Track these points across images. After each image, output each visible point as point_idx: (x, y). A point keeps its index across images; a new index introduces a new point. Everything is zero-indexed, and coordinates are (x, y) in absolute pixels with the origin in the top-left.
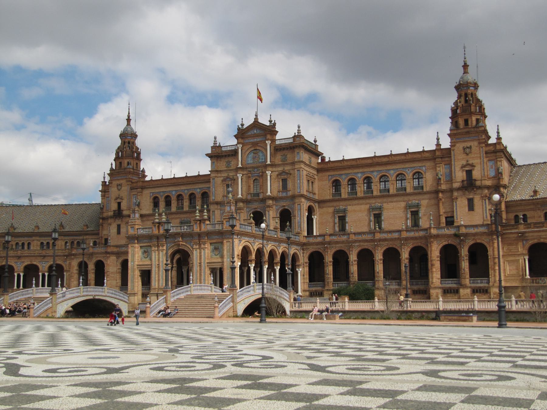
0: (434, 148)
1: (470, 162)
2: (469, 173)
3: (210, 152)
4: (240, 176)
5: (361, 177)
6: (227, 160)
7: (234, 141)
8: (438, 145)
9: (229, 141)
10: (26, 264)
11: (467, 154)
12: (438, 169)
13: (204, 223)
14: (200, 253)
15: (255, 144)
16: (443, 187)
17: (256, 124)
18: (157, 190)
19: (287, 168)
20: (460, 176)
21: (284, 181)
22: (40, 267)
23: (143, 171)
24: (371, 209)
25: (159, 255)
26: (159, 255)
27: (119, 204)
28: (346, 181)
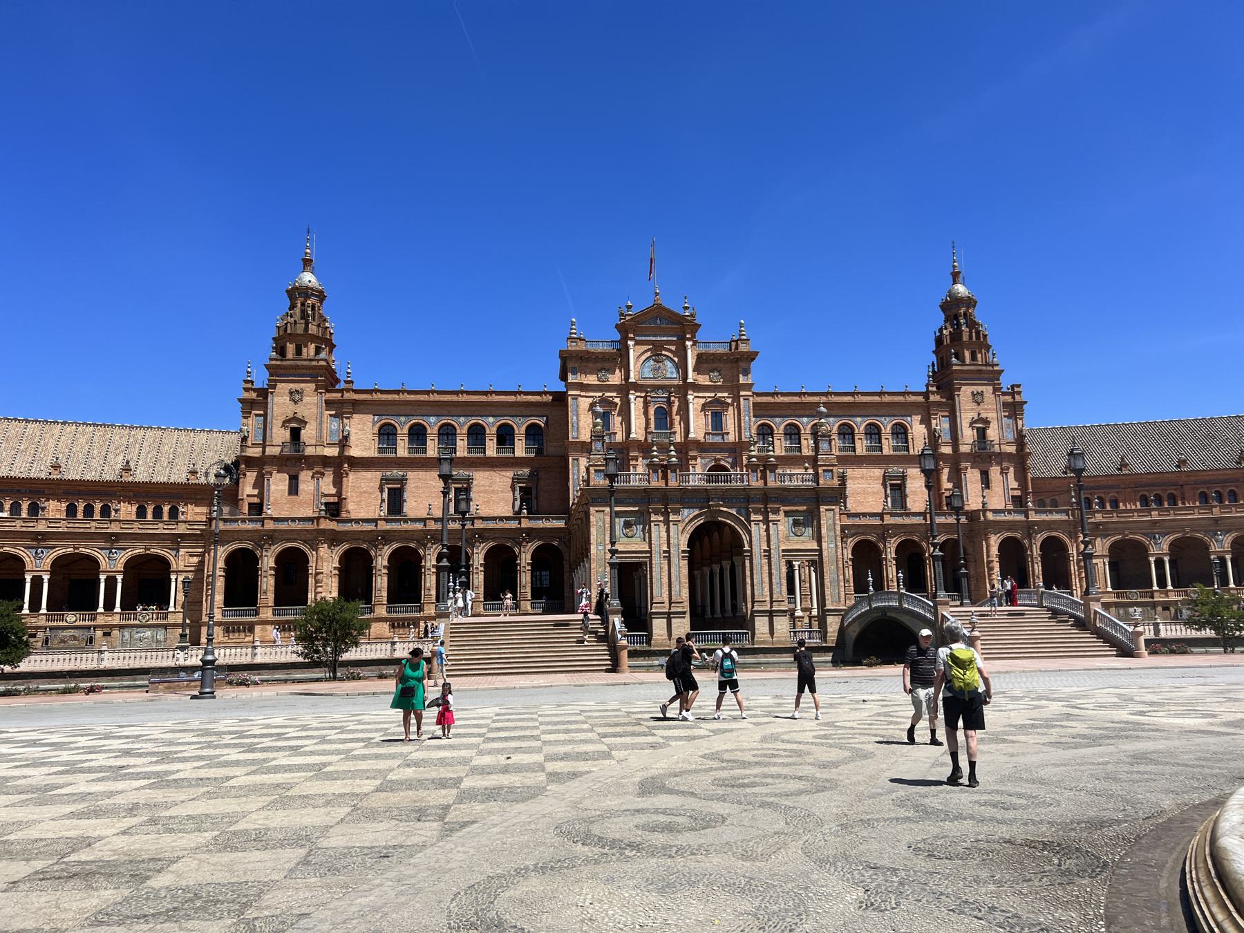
1: (983, 415)
2: (982, 434)
5: (808, 423)
7: (618, 337)
10: (61, 552)
11: (979, 404)
12: (934, 422)
13: (773, 471)
14: (767, 530)
16: (946, 450)
20: (968, 435)
22: (104, 564)
25: (668, 531)
26: (668, 531)
27: (295, 434)
28: (782, 427)
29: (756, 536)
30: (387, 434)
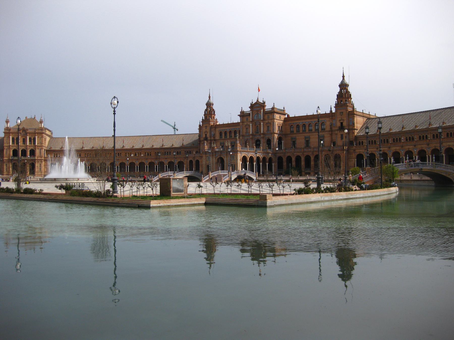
0: (329, 112)
2: (342, 123)
3: (239, 114)
4: (251, 124)
6: (246, 117)
7: (249, 110)
8: (331, 111)
9: (247, 109)
15: (258, 111)
17: (257, 103)
18: (221, 129)
19: (270, 121)
21: (268, 127)
23: (216, 120)
24: (305, 138)
27: (206, 135)
29: (225, 159)
30: (221, 134)
